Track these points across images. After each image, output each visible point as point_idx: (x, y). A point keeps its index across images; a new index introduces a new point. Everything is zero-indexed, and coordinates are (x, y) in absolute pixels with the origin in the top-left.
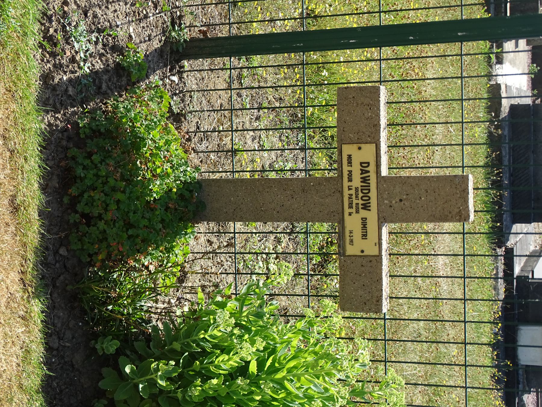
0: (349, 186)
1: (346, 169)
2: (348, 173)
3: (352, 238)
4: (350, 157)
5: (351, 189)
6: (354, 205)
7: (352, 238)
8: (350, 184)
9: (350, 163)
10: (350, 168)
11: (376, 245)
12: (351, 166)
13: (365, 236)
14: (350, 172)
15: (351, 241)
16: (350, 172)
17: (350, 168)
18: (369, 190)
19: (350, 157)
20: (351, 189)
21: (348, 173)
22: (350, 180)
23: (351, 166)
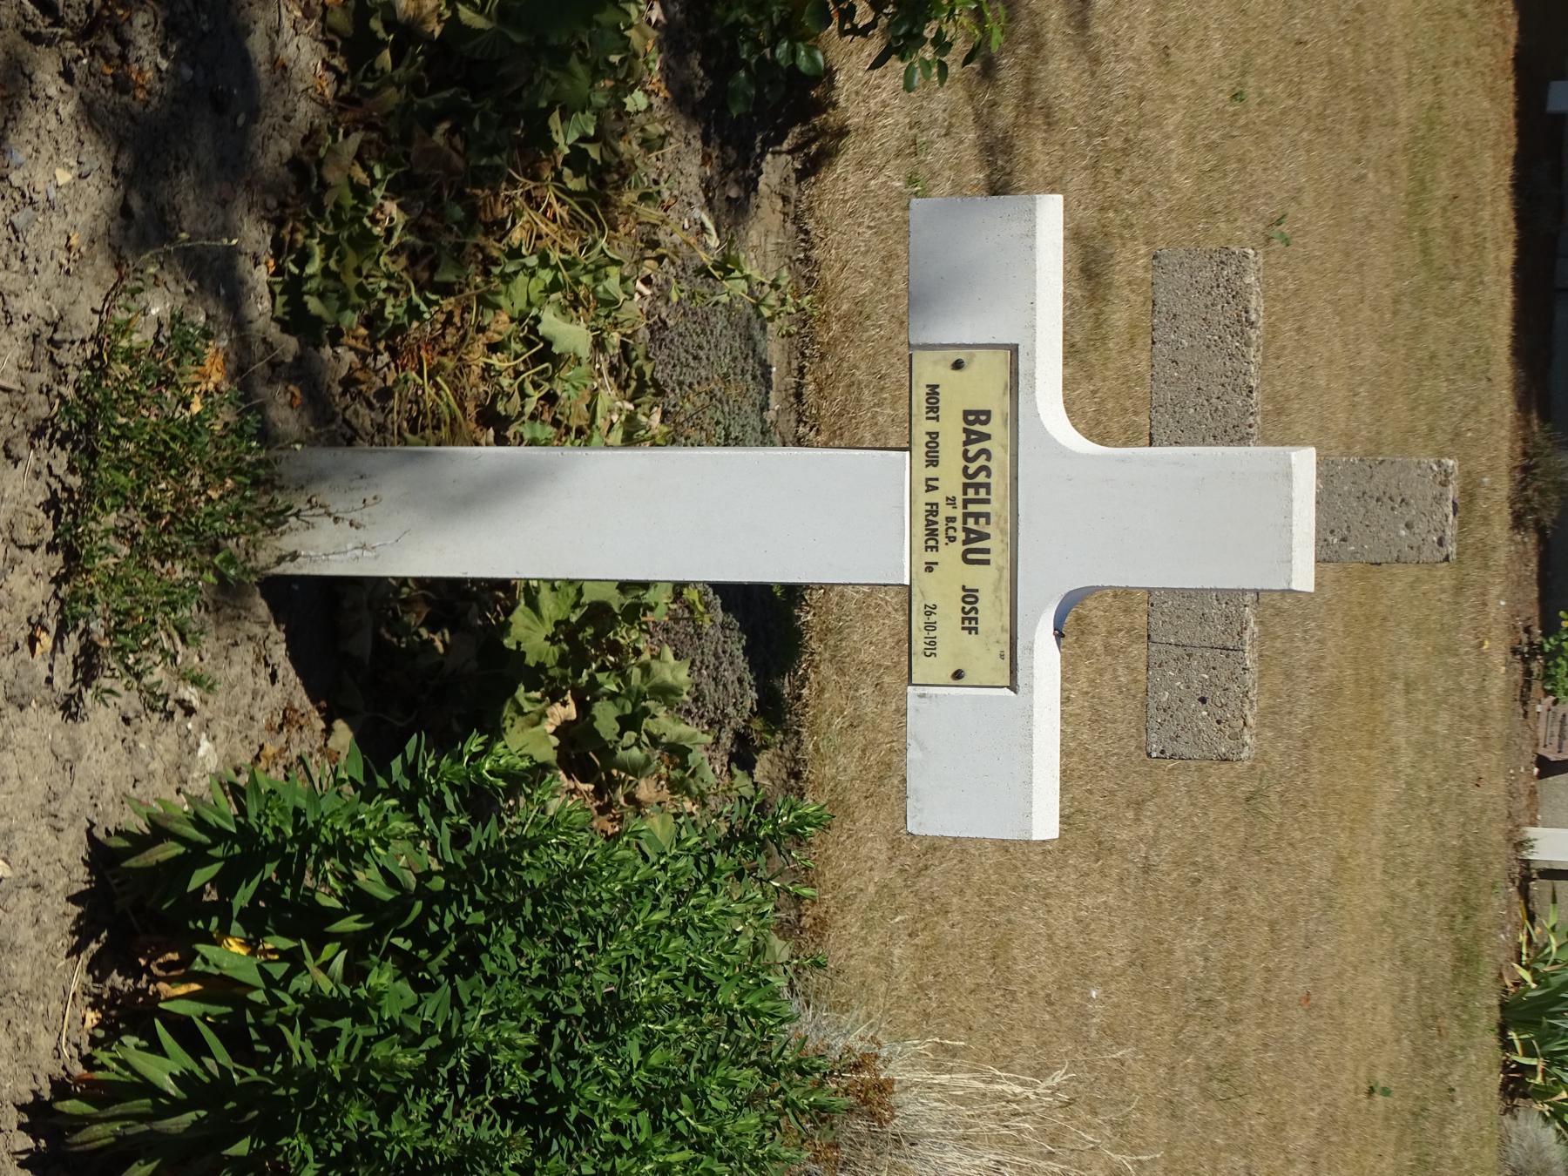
1: (922, 426)
2: (927, 438)
3: (932, 634)
4: (933, 390)
6: (942, 538)
7: (932, 634)
9: (933, 408)
10: (932, 426)
11: (1002, 657)
12: (937, 419)
13: (970, 622)
14: (933, 436)
15: (932, 643)
16: (933, 436)
17: (932, 426)
19: (933, 390)
21: (927, 438)
22: (933, 461)
23: (937, 419)
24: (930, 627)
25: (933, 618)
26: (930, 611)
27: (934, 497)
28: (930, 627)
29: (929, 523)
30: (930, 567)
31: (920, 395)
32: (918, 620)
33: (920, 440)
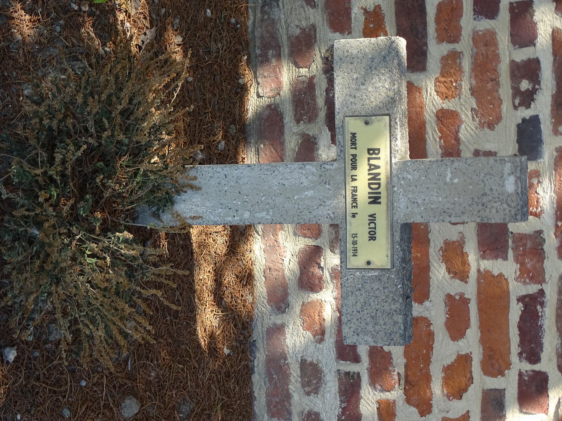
0: (352, 176)
2: (352, 157)
5: (356, 180)
7: (355, 246)
8: (354, 172)
9: (354, 143)
10: (353, 152)
12: (356, 148)
14: (354, 156)
15: (355, 250)
17: (353, 152)
18: (379, 184)
19: (354, 135)
20: (356, 180)
21: (352, 157)
23: (356, 148)
24: (355, 243)
25: (355, 239)
26: (355, 236)
27: (354, 184)
28: (355, 243)
29: (353, 195)
30: (354, 215)
31: (348, 137)
32: (349, 239)
33: (348, 159)
